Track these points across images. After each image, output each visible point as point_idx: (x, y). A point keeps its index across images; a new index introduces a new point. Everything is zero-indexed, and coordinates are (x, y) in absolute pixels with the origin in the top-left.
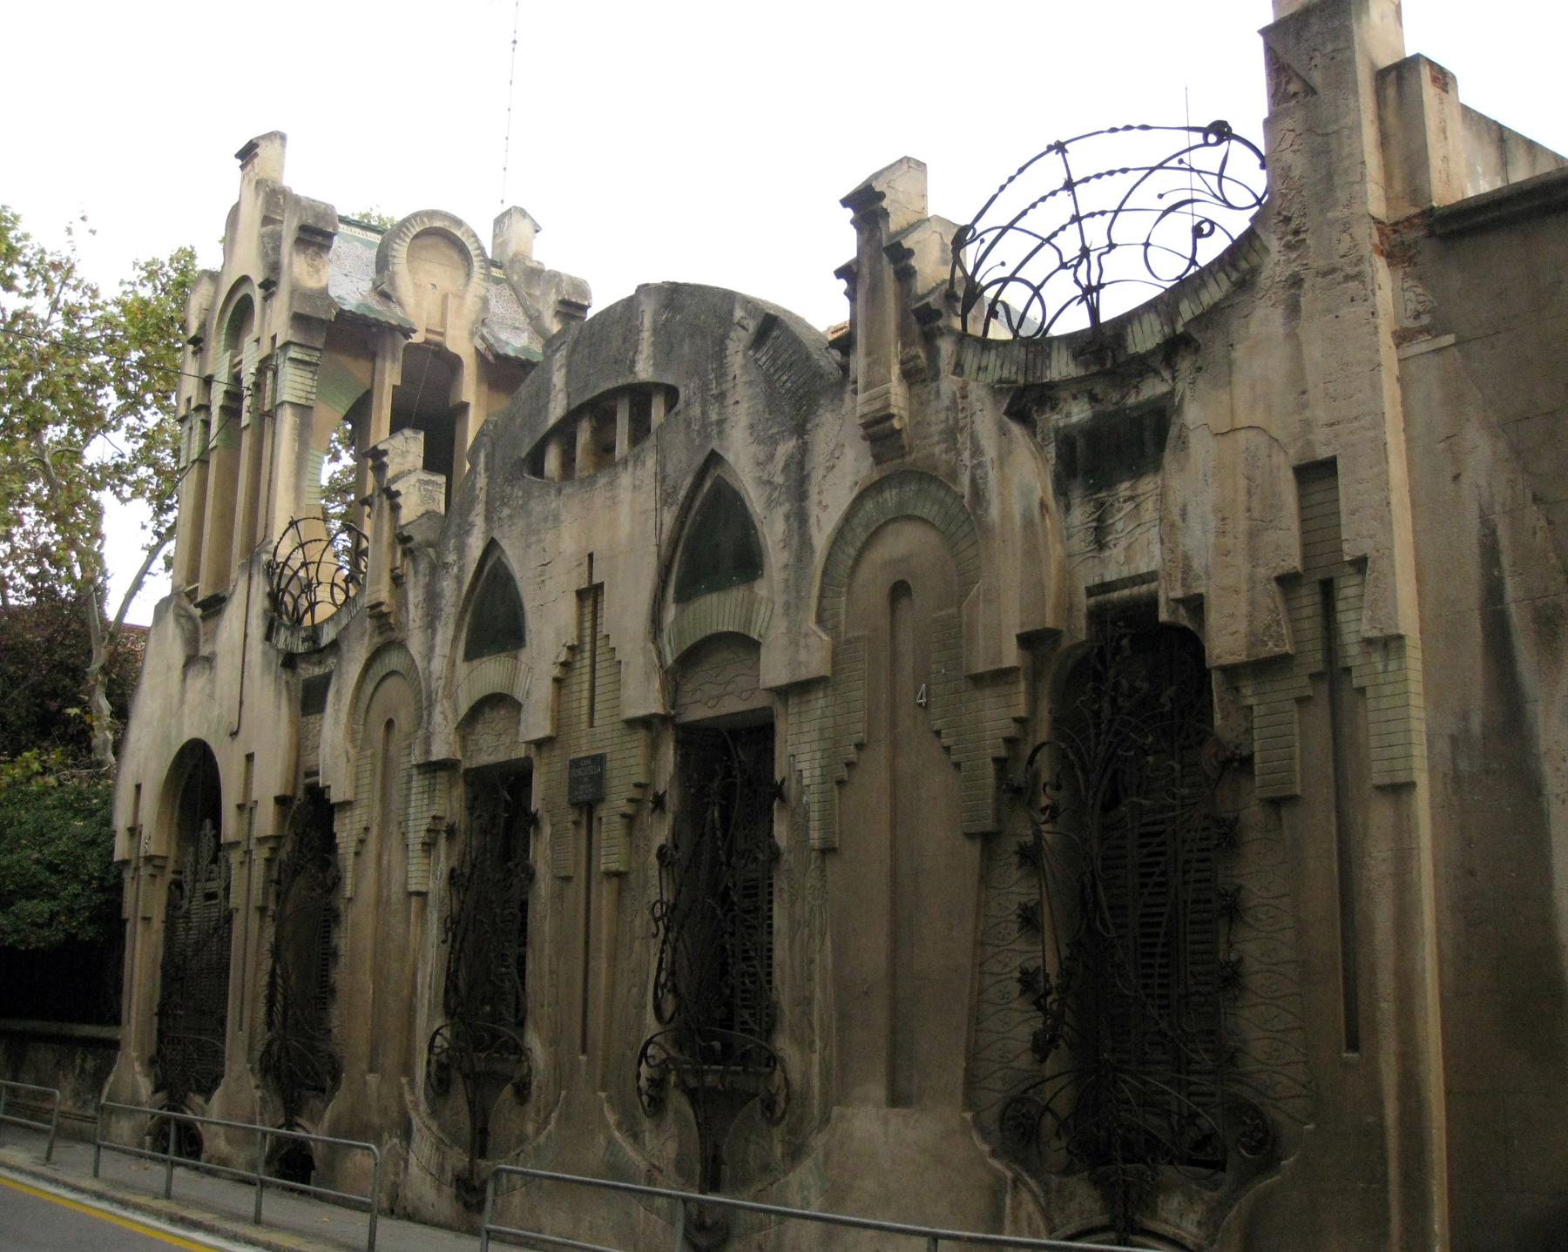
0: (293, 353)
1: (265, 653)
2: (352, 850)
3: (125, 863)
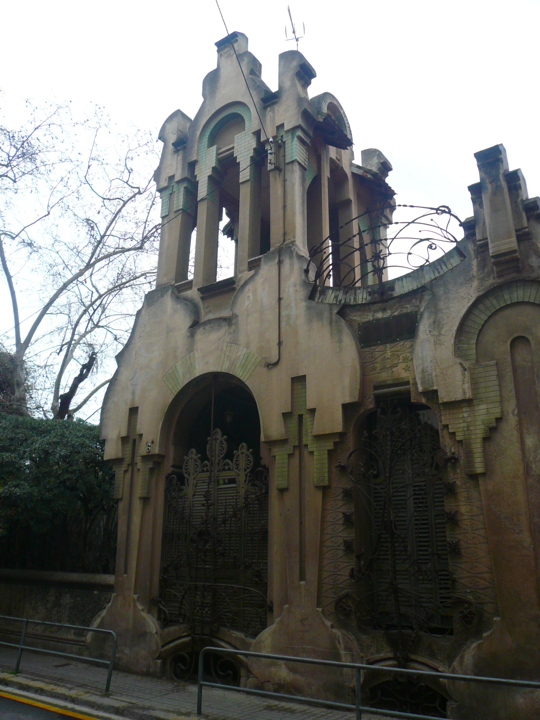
0: (299, 133)
1: (309, 308)
2: (480, 436)
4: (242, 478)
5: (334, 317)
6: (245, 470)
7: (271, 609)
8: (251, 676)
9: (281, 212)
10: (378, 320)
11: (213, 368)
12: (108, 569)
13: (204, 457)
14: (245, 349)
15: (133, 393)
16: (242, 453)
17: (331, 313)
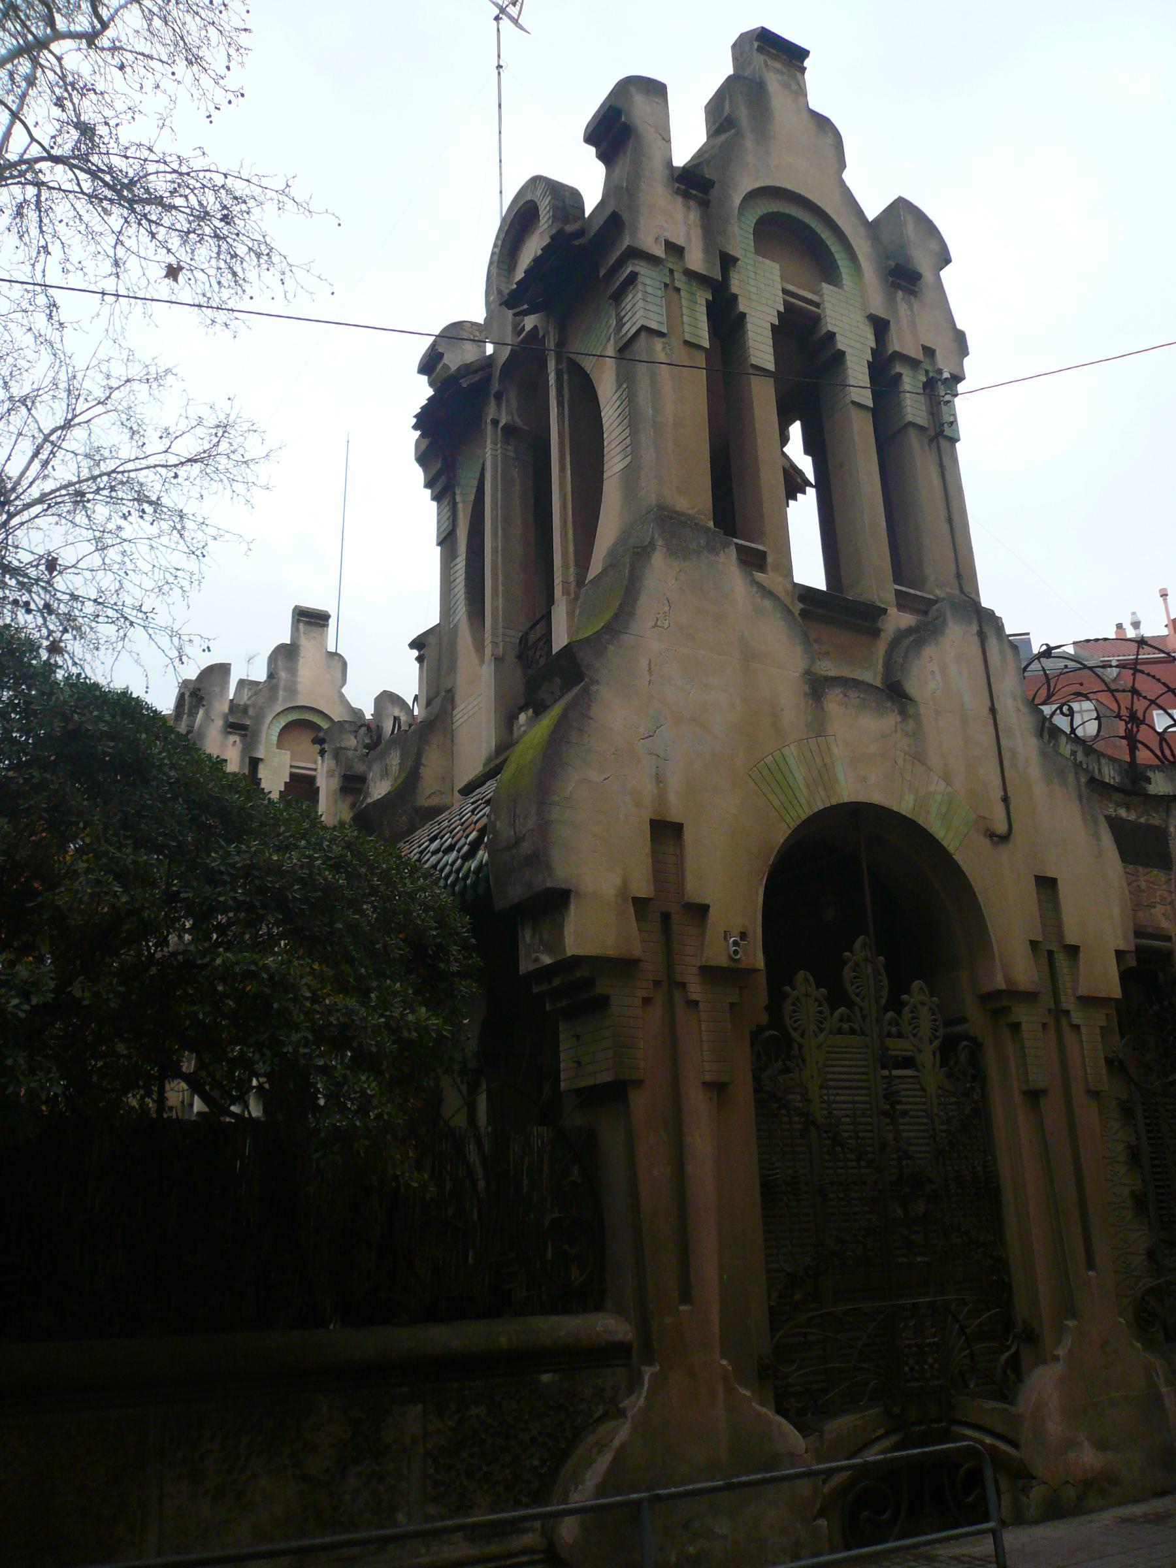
3: (623, 967)
4: (927, 1056)
5: (1083, 789)
6: (931, 1043)
7: (1031, 1337)
8: (1034, 1482)
9: (946, 527)
10: (1121, 819)
11: (877, 797)
12: (588, 1297)
13: (837, 997)
14: (942, 784)
15: (659, 779)
16: (923, 1004)
17: (1078, 780)
